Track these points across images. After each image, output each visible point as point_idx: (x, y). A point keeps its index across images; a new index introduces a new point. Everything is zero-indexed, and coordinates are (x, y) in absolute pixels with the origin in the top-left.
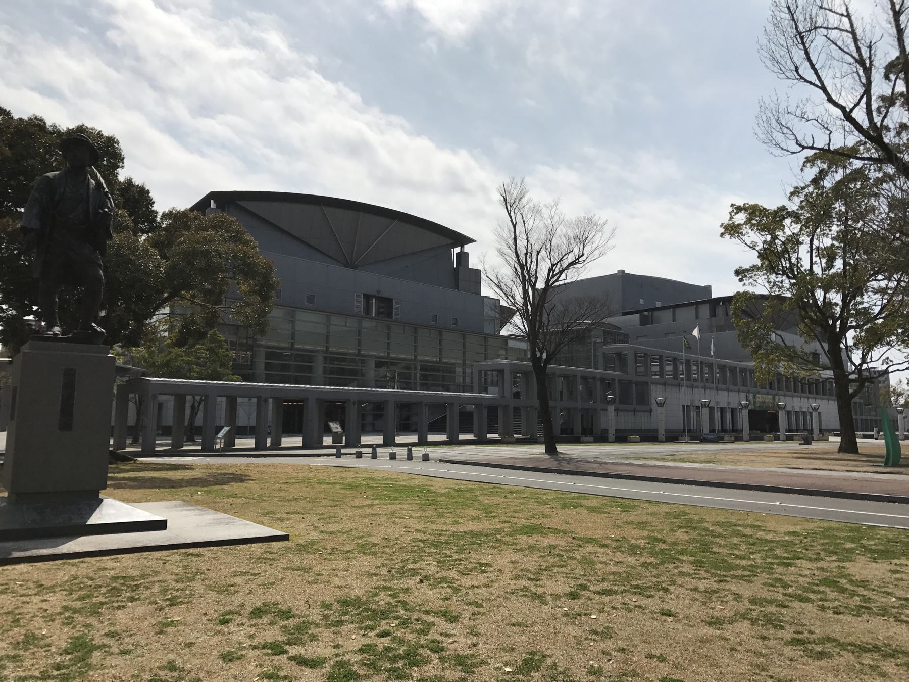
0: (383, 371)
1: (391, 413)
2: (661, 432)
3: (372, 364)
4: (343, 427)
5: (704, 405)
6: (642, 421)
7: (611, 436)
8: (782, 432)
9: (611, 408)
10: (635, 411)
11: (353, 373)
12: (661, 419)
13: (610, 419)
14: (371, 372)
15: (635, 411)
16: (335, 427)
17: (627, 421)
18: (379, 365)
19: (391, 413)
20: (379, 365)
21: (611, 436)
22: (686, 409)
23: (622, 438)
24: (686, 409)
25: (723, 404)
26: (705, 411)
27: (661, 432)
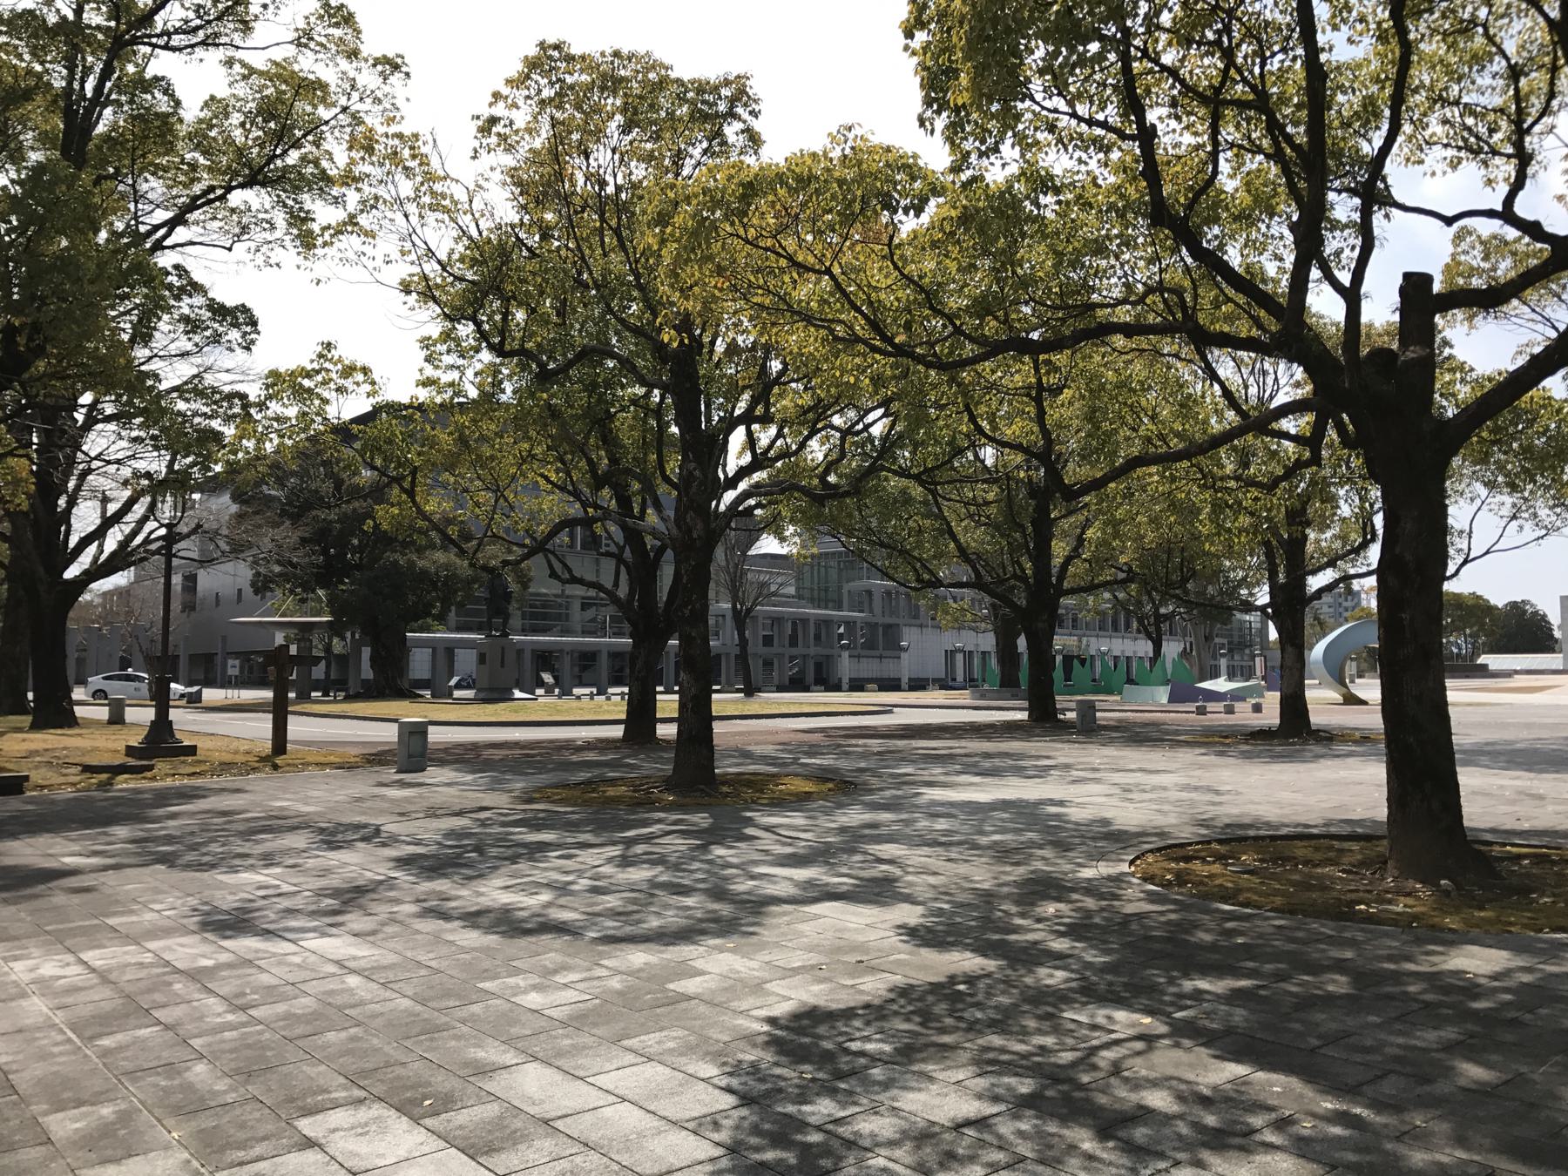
0: (591, 613)
1: (604, 662)
2: (905, 681)
3: (577, 606)
4: (555, 677)
5: (961, 650)
6: (888, 669)
7: (845, 686)
8: (528, 656)
9: (846, 654)
10: (881, 657)
11: (558, 617)
12: (906, 667)
13: (846, 666)
14: (577, 615)
15: (881, 657)
16: (548, 678)
17: (869, 668)
18: (584, 607)
19: (604, 662)
20: (584, 607)
21: (845, 686)
22: (950, 655)
23: (857, 686)
24: (950, 655)
25: (1117, 653)
26: (960, 657)
27: (905, 681)
